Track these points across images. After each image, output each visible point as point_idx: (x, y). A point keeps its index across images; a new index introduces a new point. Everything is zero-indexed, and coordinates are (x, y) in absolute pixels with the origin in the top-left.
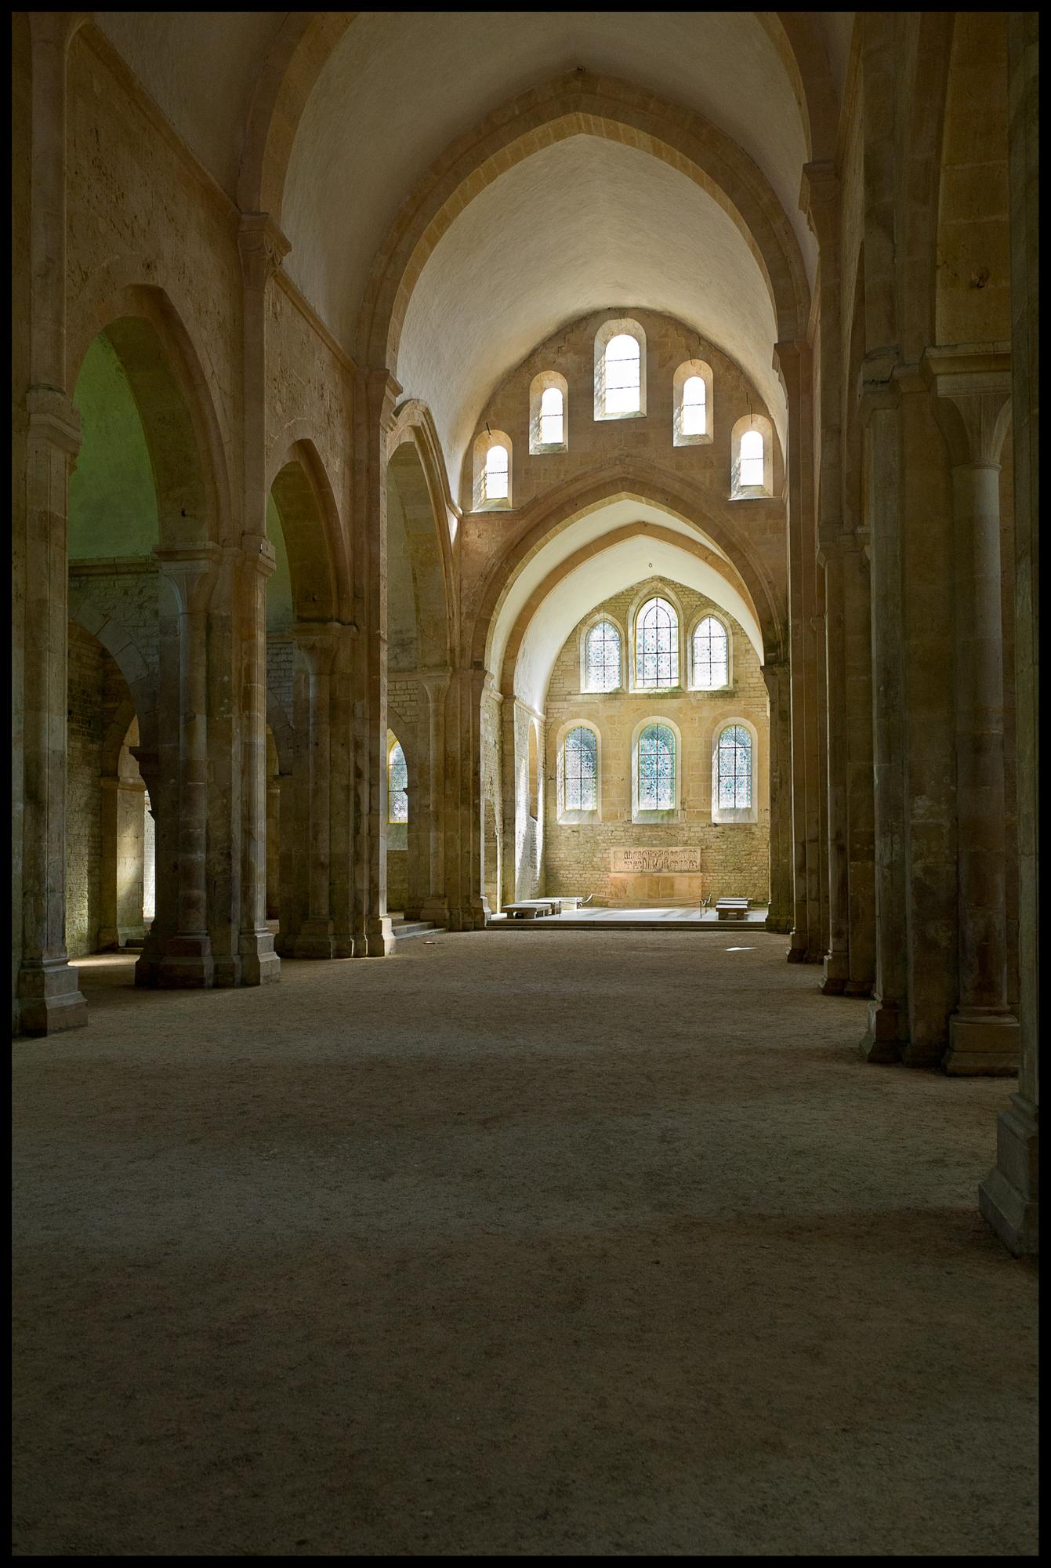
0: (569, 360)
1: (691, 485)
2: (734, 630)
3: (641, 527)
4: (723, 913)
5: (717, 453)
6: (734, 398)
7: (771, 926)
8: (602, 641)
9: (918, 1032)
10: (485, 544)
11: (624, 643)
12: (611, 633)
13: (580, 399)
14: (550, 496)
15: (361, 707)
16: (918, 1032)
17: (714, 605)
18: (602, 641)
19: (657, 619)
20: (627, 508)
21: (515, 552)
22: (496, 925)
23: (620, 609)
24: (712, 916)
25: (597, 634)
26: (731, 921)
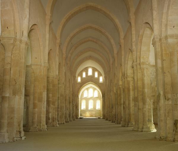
0: (86, 71)
2: (99, 91)
3: (91, 83)
4: (98, 118)
5: (98, 79)
6: (100, 74)
7: (103, 119)
9: (114, 121)
11: (88, 92)
13: (87, 74)
14: (85, 82)
15: (74, 102)
16: (114, 121)
17: (96, 89)
19: (91, 90)
23: (87, 89)
24: (97, 118)
26: (99, 118)
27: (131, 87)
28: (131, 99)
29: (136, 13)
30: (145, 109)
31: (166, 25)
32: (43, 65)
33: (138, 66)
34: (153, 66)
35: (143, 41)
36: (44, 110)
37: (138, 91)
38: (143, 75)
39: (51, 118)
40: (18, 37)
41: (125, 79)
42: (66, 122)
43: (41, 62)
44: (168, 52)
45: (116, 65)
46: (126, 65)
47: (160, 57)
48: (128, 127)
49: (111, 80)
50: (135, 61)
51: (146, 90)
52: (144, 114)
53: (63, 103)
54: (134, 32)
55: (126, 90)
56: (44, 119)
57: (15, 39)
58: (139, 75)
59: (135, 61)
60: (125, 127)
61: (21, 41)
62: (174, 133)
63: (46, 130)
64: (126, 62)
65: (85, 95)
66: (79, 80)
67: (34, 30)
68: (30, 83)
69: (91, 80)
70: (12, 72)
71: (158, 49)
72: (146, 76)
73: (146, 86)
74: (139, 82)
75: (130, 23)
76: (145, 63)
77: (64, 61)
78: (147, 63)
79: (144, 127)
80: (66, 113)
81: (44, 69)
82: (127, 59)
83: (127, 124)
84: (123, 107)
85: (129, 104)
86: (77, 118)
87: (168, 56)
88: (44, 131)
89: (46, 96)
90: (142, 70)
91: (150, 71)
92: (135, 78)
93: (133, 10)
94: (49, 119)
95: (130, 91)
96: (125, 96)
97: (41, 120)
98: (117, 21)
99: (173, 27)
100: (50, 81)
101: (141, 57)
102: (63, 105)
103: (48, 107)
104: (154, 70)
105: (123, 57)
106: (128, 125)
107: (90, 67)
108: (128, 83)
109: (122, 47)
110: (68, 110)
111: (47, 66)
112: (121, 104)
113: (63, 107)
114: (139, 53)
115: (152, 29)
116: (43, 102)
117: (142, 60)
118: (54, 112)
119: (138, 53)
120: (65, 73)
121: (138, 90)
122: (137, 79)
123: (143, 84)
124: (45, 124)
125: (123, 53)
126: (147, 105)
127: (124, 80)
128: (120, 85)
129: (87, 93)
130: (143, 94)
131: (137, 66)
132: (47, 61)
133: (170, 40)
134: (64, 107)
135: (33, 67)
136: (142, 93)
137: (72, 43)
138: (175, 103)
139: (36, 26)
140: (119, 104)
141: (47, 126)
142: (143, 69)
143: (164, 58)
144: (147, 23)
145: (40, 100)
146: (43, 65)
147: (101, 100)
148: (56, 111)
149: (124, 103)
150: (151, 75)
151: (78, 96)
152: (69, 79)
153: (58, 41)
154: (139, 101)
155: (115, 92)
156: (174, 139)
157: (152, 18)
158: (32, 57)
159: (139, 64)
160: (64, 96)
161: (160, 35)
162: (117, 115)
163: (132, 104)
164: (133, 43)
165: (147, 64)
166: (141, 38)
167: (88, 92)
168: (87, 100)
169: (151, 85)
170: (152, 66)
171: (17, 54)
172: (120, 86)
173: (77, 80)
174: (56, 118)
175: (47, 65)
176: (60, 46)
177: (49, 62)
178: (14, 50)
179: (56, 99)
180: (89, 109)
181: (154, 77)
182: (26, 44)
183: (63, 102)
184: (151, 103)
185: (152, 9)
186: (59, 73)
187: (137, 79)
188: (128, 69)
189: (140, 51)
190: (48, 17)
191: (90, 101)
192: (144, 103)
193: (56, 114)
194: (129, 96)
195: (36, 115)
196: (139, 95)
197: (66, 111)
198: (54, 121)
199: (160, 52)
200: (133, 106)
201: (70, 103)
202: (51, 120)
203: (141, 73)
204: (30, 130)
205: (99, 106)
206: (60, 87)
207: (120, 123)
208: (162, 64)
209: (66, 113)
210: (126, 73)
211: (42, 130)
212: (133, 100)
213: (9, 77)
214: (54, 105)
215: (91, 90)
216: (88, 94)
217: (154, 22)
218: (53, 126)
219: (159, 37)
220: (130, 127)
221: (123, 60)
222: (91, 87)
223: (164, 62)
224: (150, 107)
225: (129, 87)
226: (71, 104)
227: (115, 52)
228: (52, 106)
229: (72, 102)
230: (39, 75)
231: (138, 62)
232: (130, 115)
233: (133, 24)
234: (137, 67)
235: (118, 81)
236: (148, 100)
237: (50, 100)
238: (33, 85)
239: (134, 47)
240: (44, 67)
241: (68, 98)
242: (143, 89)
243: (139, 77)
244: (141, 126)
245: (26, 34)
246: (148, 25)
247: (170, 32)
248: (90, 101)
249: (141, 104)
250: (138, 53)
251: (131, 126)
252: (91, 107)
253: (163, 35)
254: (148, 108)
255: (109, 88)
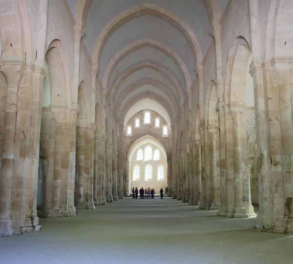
1: (156, 134)
5: (161, 130)
8: (140, 151)
9: (186, 200)
10: (128, 141)
11: (144, 153)
12: (142, 151)
13: (142, 121)
14: (137, 136)
15: (120, 168)
16: (186, 200)
17: (157, 147)
18: (140, 152)
19: (148, 149)
20: (148, 136)
21: (132, 143)
22: (129, 196)
23: (143, 148)
25: (139, 151)
27: (214, 144)
28: (215, 164)
29: (223, 21)
30: (238, 181)
31: (273, 41)
32: (71, 107)
33: (227, 109)
34: (251, 108)
35: (234, 67)
36: (71, 181)
37: (226, 151)
38: (234, 123)
39: (82, 193)
40: (29, 61)
41: (204, 130)
42: (108, 202)
43: (66, 102)
44: (275, 86)
45: (190, 107)
46: (206, 107)
47: (263, 93)
48: (209, 209)
49: (182, 132)
50: (221, 100)
51: (239, 149)
52: (235, 188)
53: (103, 170)
54: (219, 52)
55: (206, 148)
56: (71, 197)
57: (24, 65)
58: (229, 124)
59: (221, 100)
60: (205, 209)
61: (33, 67)
62: (286, 219)
63: (75, 214)
64: (207, 102)
65: (139, 157)
66: (129, 131)
67: (54, 49)
68: (48, 137)
69: (149, 132)
70: (18, 118)
71: (260, 80)
72: (239, 126)
73: (239, 142)
74: (227, 136)
75: (213, 37)
76: (238, 104)
77: (104, 101)
78: (242, 104)
79: (236, 209)
80: (107, 188)
81: (71, 114)
82: (208, 96)
83: (207, 205)
84: (202, 176)
85: (211, 172)
86: (125, 195)
87: (275, 91)
88: (71, 216)
89: (75, 158)
90: (232, 115)
91: (246, 117)
92: (221, 129)
93: (217, 16)
94: (80, 197)
95: (213, 150)
96: (205, 158)
97: (67, 198)
98: (191, 34)
99: (283, 44)
100: (82, 133)
101: (232, 93)
102: (103, 173)
103: (77, 176)
104: (253, 115)
105: (201, 93)
106: (210, 206)
107: (148, 110)
108: (210, 137)
109: (200, 77)
110: (110, 181)
111: (77, 108)
112: (199, 172)
113: (103, 176)
114: (228, 88)
115: (249, 47)
116: (70, 168)
117: (233, 99)
118: (88, 186)
119: (227, 88)
120: (106, 119)
121: (226, 148)
122: (225, 130)
123: (235, 139)
124: (73, 205)
125: (201, 86)
126: (241, 174)
127: (202, 132)
128: (197, 140)
129: (142, 153)
130: (235, 154)
131: (224, 109)
132: (76, 101)
133: (279, 66)
134: (105, 177)
135: (53, 110)
136: (232, 153)
137: (117, 71)
138: (288, 170)
139: (58, 42)
140: (194, 171)
141: (77, 209)
142: (235, 114)
143: (270, 96)
144: (241, 37)
145: (65, 165)
146: (70, 106)
147: (165, 167)
148: (91, 182)
149: (203, 170)
150: (248, 124)
151: (127, 158)
152: (113, 130)
153: (95, 67)
154: (228, 166)
155: (188, 151)
156: (287, 229)
157: (250, 28)
158: (51, 93)
159: (229, 105)
160: (105, 158)
161: (263, 58)
162: (192, 190)
163: (216, 172)
164: (217, 71)
165: (240, 106)
166: (231, 63)
167: (144, 153)
168: (142, 164)
169: (247, 140)
170: (249, 108)
171: (26, 89)
172: (196, 142)
173: (125, 131)
174: (91, 196)
175: (76, 106)
176: (97, 75)
177: (79, 102)
178: (22, 82)
179: (91, 164)
180: (146, 180)
181: (252, 126)
182: (43, 72)
183: (103, 168)
184: (249, 170)
185: (249, 15)
186: (96, 120)
187: (225, 130)
188: (209, 113)
189: (229, 83)
190: (78, 27)
191: (148, 167)
192: (236, 169)
193: (91, 189)
194: (212, 158)
195: (59, 190)
196: (227, 156)
197: (108, 184)
198: (87, 200)
199: (263, 85)
200: (218, 175)
201: (113, 169)
202: (82, 198)
203: (232, 120)
204: (48, 216)
205: (162, 175)
206: (99, 143)
207: (197, 202)
208: (267, 106)
209: (107, 188)
210: (206, 120)
211: (68, 214)
212: (217, 165)
213: (15, 127)
214: (88, 174)
215: (148, 149)
216: (144, 155)
217: (253, 35)
218: (87, 208)
219: (261, 61)
220: (213, 209)
221: (201, 98)
222: (148, 144)
223: (269, 101)
224: (245, 177)
225: (212, 143)
226: (116, 172)
227: (189, 85)
228: (84, 175)
229: (118, 168)
230: (64, 122)
231: (227, 102)
232: (212, 189)
233: (218, 39)
234: (224, 110)
235: (193, 133)
236: (242, 165)
237: (81, 165)
238: (53, 141)
239: (219, 77)
240: (72, 110)
241: (110, 162)
242: (234, 146)
243: (227, 128)
244: (231, 208)
245: (41, 55)
246: (243, 41)
247: (279, 52)
248: (148, 167)
249: (231, 172)
250: (227, 88)
251: (215, 207)
252: (148, 176)
253: (268, 57)
254: (243, 179)
255: (178, 146)
